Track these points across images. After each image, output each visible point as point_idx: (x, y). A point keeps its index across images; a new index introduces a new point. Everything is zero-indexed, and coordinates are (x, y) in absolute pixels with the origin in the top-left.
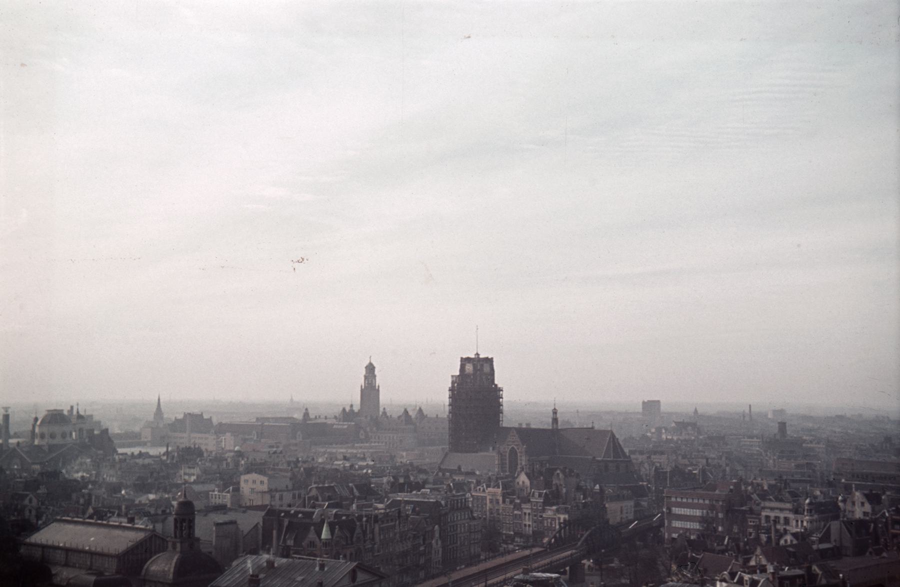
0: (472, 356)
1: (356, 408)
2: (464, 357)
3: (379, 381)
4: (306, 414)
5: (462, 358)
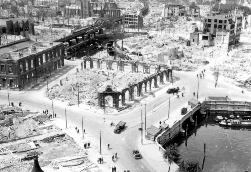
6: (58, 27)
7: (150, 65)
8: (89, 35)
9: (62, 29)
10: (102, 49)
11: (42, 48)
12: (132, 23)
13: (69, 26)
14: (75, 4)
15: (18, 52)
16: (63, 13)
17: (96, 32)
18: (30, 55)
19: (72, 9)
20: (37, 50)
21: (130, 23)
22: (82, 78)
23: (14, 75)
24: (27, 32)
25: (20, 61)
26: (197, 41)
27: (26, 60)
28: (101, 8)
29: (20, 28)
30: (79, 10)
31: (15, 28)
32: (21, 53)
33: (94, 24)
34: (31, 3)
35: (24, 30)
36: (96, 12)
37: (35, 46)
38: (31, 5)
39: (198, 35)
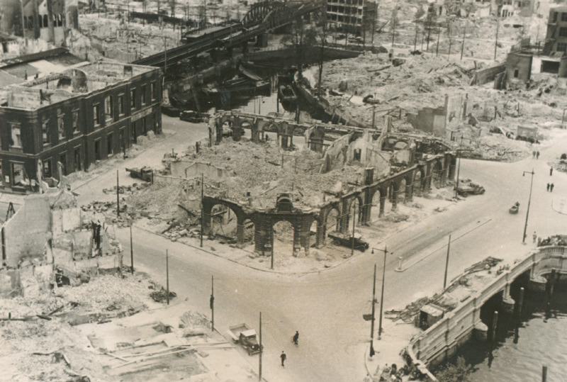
6: (145, 21)
7: (395, 140)
8: (230, 49)
9: (154, 29)
10: (266, 92)
11: (104, 80)
12: (347, 19)
13: (175, 21)
15: (38, 88)
17: (250, 40)
18: (70, 97)
20: (88, 83)
21: (341, 18)
22: (211, 167)
23: (24, 152)
24: (59, 31)
25: (42, 112)
26: (526, 76)
27: (59, 111)
29: (40, 16)
31: (25, 18)
32: (44, 90)
33: (244, 19)
35: (50, 23)
37: (83, 74)
39: (531, 58)
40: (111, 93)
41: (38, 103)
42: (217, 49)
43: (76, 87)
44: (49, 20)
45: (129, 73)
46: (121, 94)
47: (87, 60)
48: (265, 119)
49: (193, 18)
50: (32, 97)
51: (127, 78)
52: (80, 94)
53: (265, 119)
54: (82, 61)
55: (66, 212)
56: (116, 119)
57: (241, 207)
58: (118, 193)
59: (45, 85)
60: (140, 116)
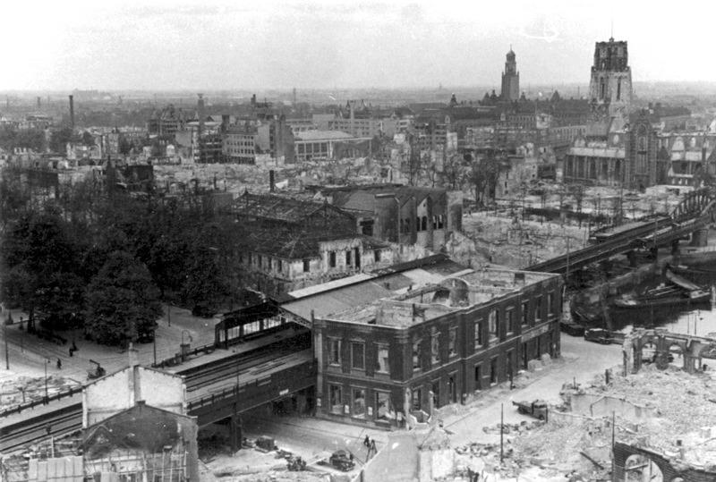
0: (607, 41)
1: (498, 93)
2: (599, 41)
3: (519, 68)
4: (454, 99)
5: (597, 43)
6: (544, 218)
8: (654, 250)
9: (554, 227)
11: (489, 291)
13: (581, 217)
14: (604, 138)
15: (410, 301)
16: (560, 173)
17: (685, 239)
18: (448, 312)
19: (593, 159)
20: (470, 295)
22: (626, 403)
24: (439, 233)
25: (415, 330)
27: (434, 329)
28: (704, 156)
29: (418, 219)
30: (618, 162)
31: (402, 220)
32: (418, 304)
33: (674, 212)
34: (455, 139)
35: (428, 226)
36: (682, 166)
37: (464, 284)
38: (456, 143)
40: (497, 306)
41: (410, 320)
42: (636, 250)
43: (455, 300)
44: (428, 222)
45: (521, 281)
46: (510, 308)
47: (469, 267)
48: (703, 342)
49: (606, 212)
50: (402, 313)
51: (518, 288)
52: (460, 308)
53: (703, 342)
54: (463, 268)
55: (436, 455)
56: (503, 338)
57: (668, 461)
58: (502, 433)
59: (419, 298)
60: (533, 335)
